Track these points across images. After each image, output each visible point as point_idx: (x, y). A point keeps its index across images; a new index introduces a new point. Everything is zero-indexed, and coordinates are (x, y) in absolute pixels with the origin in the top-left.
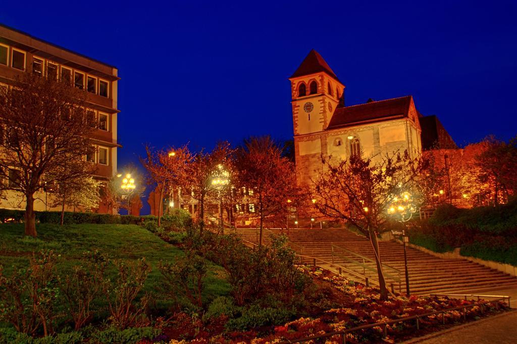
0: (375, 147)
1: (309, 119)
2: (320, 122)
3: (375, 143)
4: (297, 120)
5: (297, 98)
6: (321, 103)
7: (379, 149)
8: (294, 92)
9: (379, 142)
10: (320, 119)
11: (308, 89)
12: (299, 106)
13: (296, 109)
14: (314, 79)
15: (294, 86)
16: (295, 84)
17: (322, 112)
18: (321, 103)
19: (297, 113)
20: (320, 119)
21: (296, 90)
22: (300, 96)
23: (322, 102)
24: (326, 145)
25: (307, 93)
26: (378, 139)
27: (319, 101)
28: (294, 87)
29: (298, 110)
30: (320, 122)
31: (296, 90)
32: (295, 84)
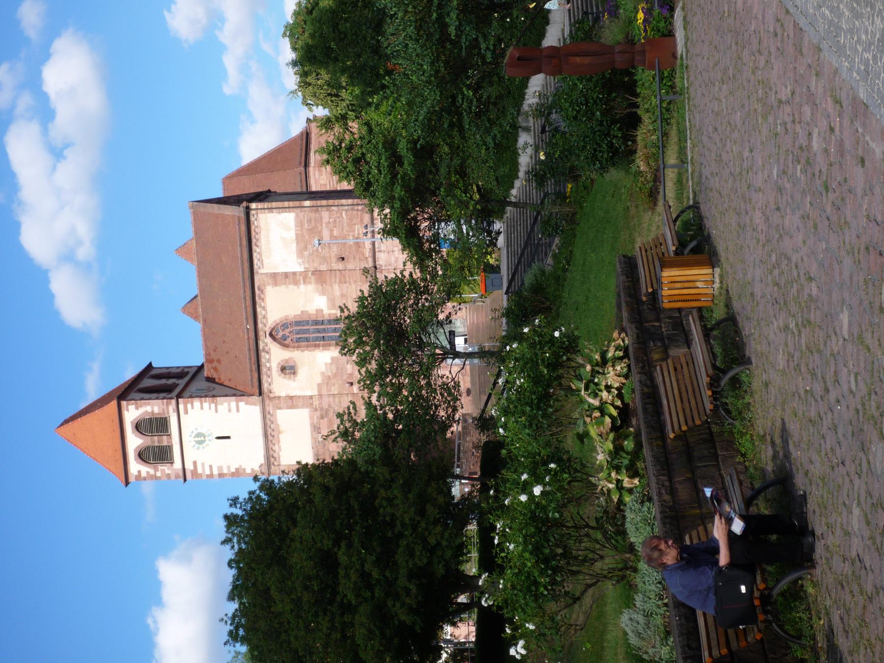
0: (304, 282)
1: (228, 438)
2: (238, 410)
3: (296, 283)
4: (229, 467)
5: (177, 464)
6: (193, 408)
7: (310, 274)
9: (294, 273)
10: (230, 410)
11: (155, 441)
12: (195, 463)
13: (200, 471)
15: (144, 474)
16: (139, 472)
17: (213, 405)
18: (193, 408)
19: (211, 467)
20: (230, 410)
21: (156, 470)
22: (172, 462)
23: (189, 406)
24: (291, 398)
25: (165, 443)
26: (286, 275)
27: (186, 412)
28: (148, 472)
29: (203, 464)
30: (238, 410)
31: (156, 470)
32: (139, 472)
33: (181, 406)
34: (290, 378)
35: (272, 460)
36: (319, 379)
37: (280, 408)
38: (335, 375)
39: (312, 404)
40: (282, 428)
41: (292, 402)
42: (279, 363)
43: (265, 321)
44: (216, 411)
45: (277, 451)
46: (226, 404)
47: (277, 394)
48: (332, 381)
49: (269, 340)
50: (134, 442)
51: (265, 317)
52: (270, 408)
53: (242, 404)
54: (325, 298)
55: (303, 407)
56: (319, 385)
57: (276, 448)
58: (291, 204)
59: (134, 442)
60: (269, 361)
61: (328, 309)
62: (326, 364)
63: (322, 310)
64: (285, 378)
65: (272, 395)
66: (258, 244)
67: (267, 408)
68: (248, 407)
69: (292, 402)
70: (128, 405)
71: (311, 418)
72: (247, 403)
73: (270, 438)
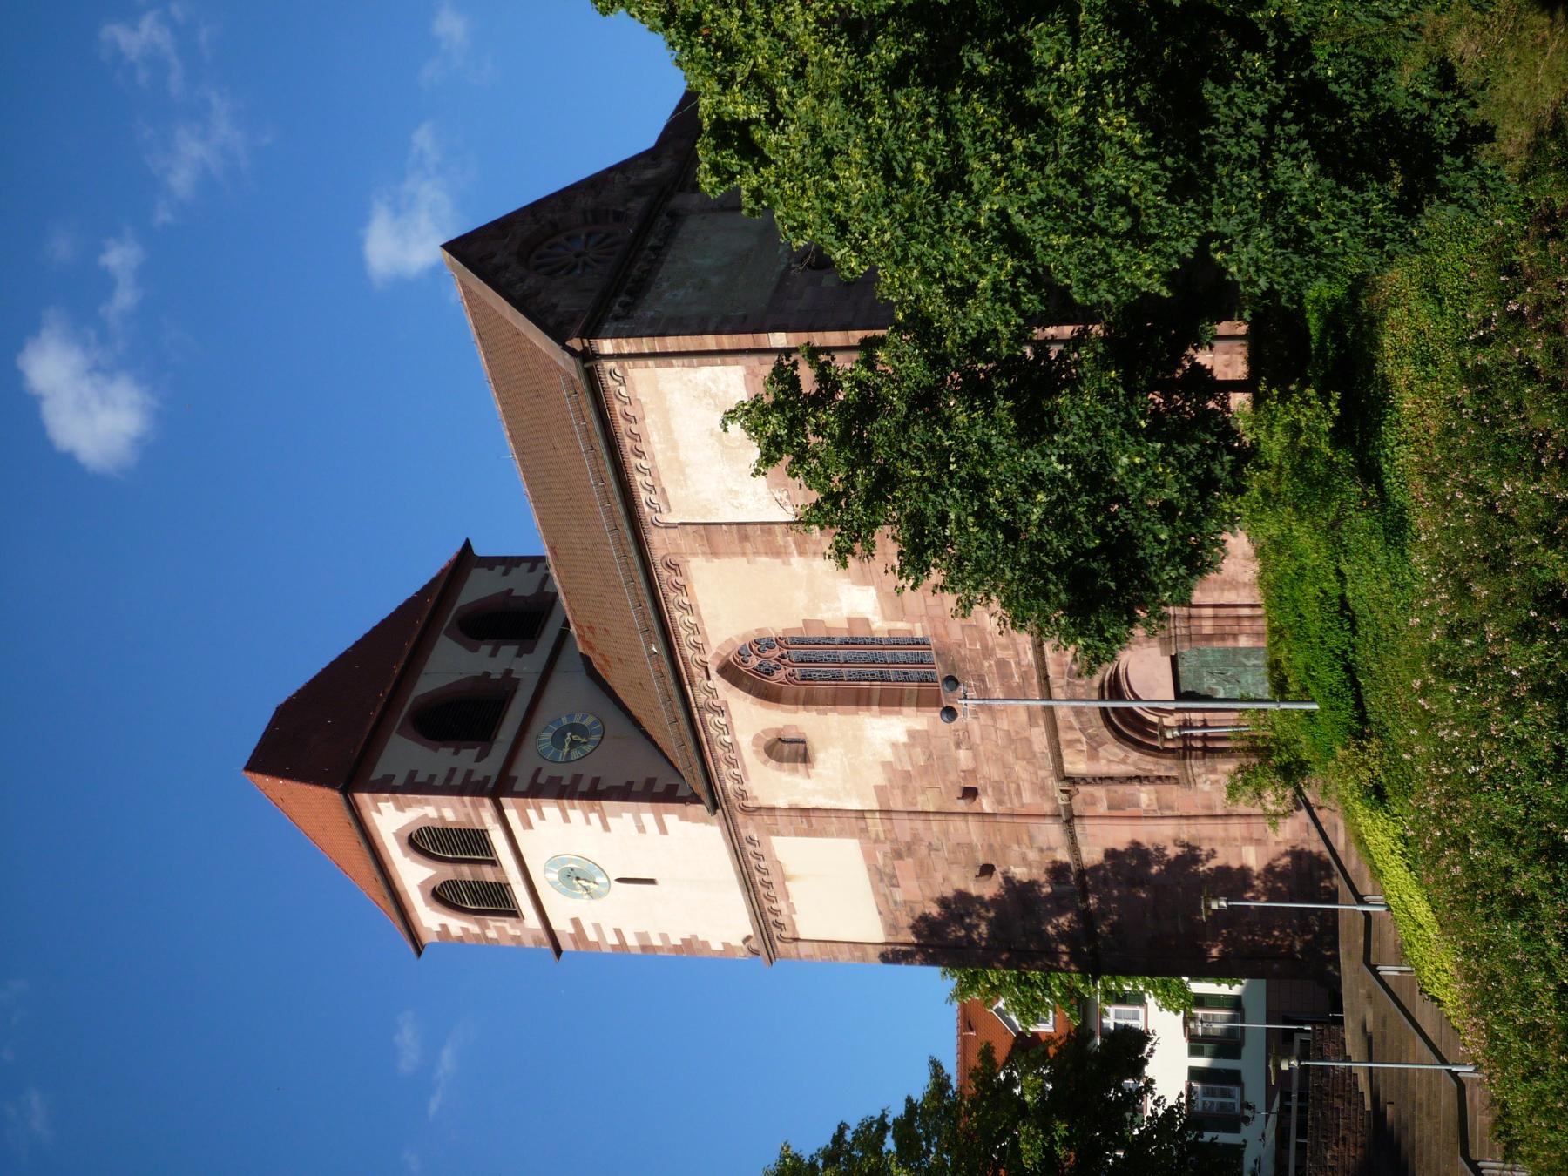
0: (801, 553)
1: (652, 882)
2: (663, 829)
4: (664, 937)
5: (531, 920)
6: (542, 817)
8: (491, 934)
14: (397, 835)
17: (594, 817)
18: (542, 817)
23: (532, 813)
27: (528, 824)
29: (597, 927)
30: (663, 829)
33: (512, 815)
34: (796, 770)
35: (775, 932)
36: (879, 779)
37: (779, 834)
38: (925, 770)
39: (865, 830)
40: (790, 869)
41: (807, 819)
42: (757, 738)
43: (699, 639)
44: (606, 827)
45: (785, 911)
46: (628, 817)
47: (765, 802)
48: (917, 784)
49: (718, 683)
50: (413, 874)
51: (695, 629)
52: (749, 829)
53: (671, 820)
54: (872, 590)
55: (841, 833)
56: (880, 790)
57: (781, 905)
58: (727, 341)
59: (413, 874)
60: (728, 728)
61: (885, 618)
62: (894, 745)
63: (866, 622)
64: (780, 769)
65: (749, 803)
66: (642, 447)
67: (744, 833)
68: (688, 825)
69: (807, 819)
70: (375, 802)
71: (868, 856)
72: (683, 818)
73: (763, 890)
